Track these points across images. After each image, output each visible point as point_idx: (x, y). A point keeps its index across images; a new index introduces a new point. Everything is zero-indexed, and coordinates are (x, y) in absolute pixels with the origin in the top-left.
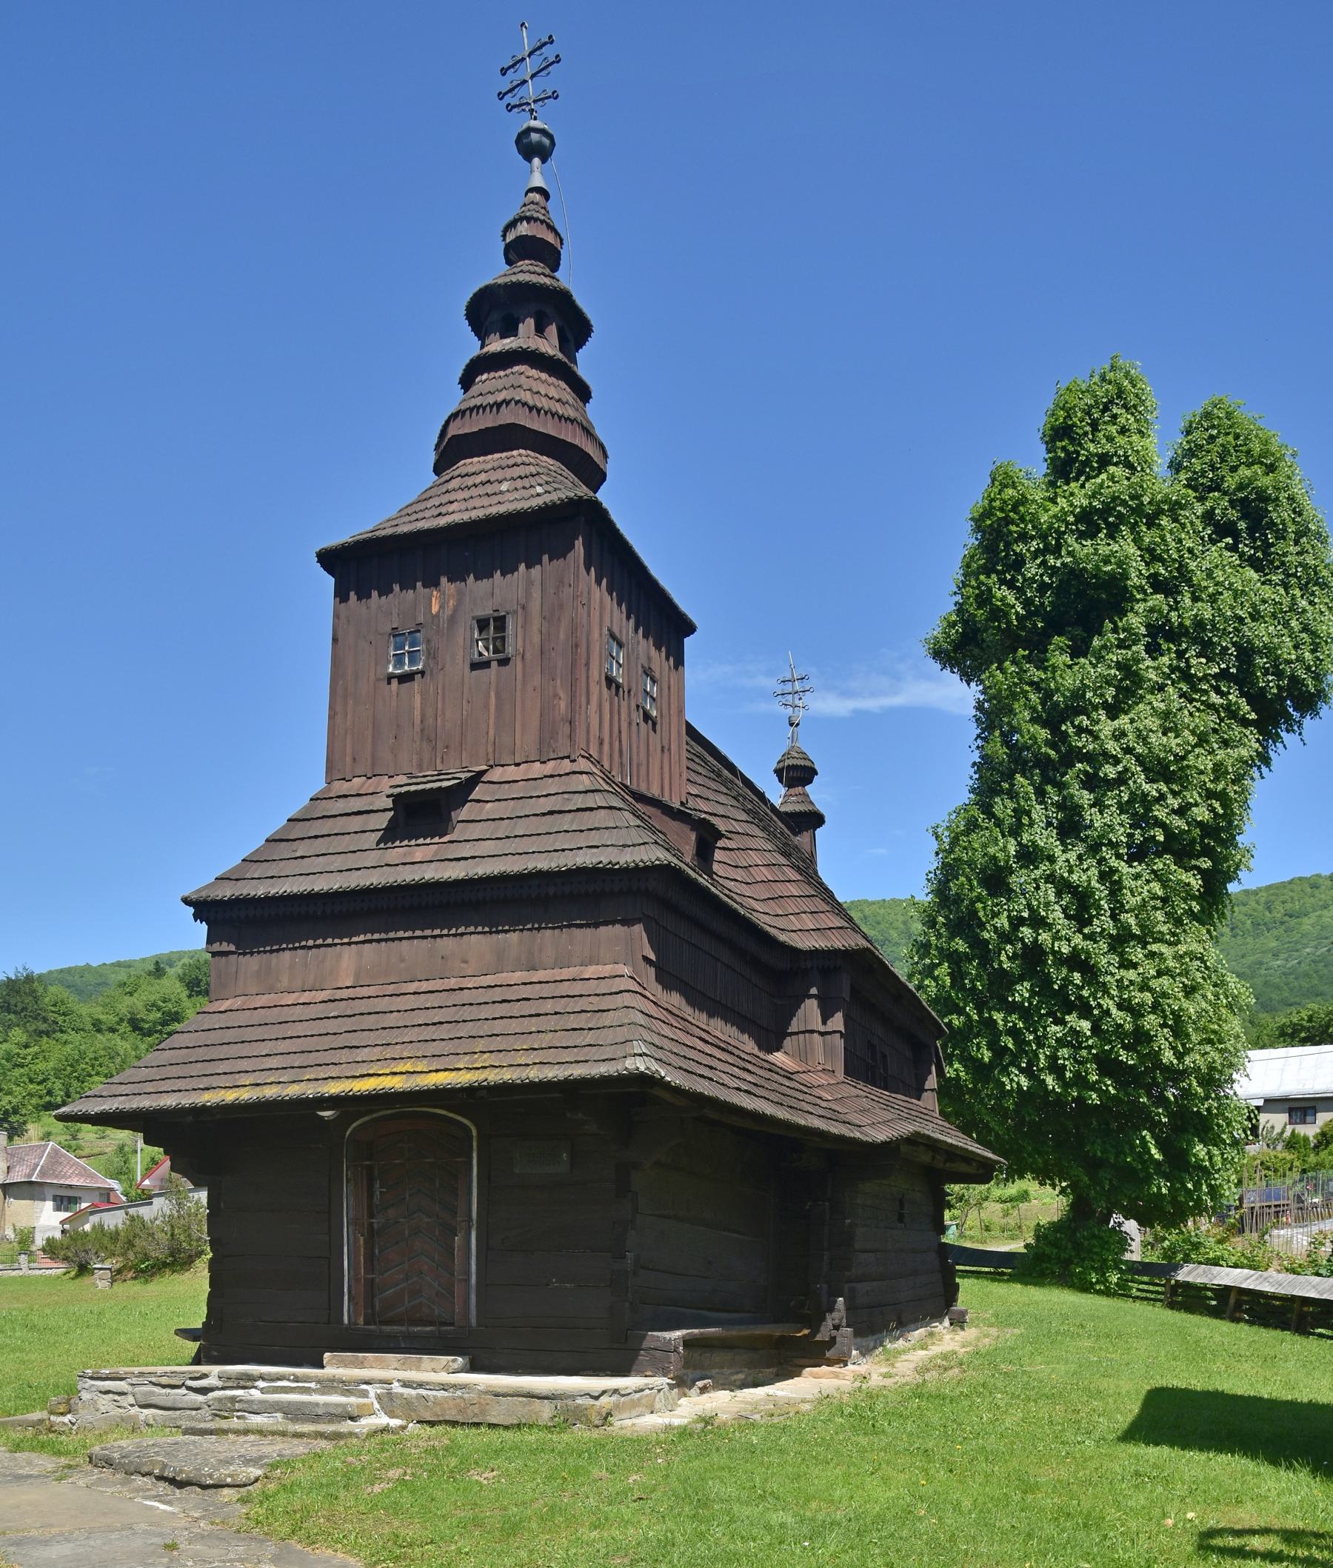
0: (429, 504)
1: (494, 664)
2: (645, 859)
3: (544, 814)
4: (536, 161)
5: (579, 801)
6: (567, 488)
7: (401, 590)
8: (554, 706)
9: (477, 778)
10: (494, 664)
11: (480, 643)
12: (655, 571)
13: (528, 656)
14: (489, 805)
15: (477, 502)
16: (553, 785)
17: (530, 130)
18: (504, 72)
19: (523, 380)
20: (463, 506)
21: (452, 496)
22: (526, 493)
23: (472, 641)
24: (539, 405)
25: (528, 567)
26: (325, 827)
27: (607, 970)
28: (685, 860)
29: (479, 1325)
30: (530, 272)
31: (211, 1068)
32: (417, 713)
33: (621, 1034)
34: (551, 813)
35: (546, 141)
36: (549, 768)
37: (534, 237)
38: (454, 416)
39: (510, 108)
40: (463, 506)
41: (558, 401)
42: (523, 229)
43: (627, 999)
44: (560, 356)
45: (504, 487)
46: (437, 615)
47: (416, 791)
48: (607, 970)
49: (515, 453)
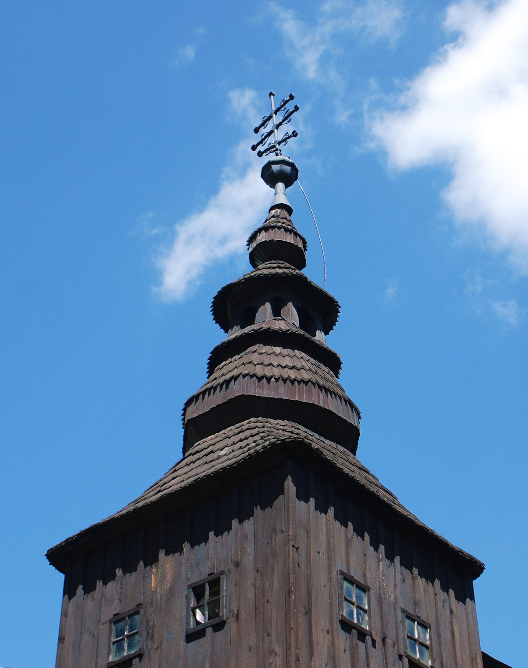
1: (209, 631)
4: (280, 186)
7: (124, 573)
8: (271, 664)
10: (209, 631)
11: (198, 612)
13: (243, 615)
17: (270, 164)
18: (256, 130)
23: (187, 609)
24: (268, 374)
25: (241, 522)
35: (288, 169)
37: (272, 241)
38: (188, 403)
41: (293, 368)
42: (262, 237)
44: (302, 332)
49: (244, 423)
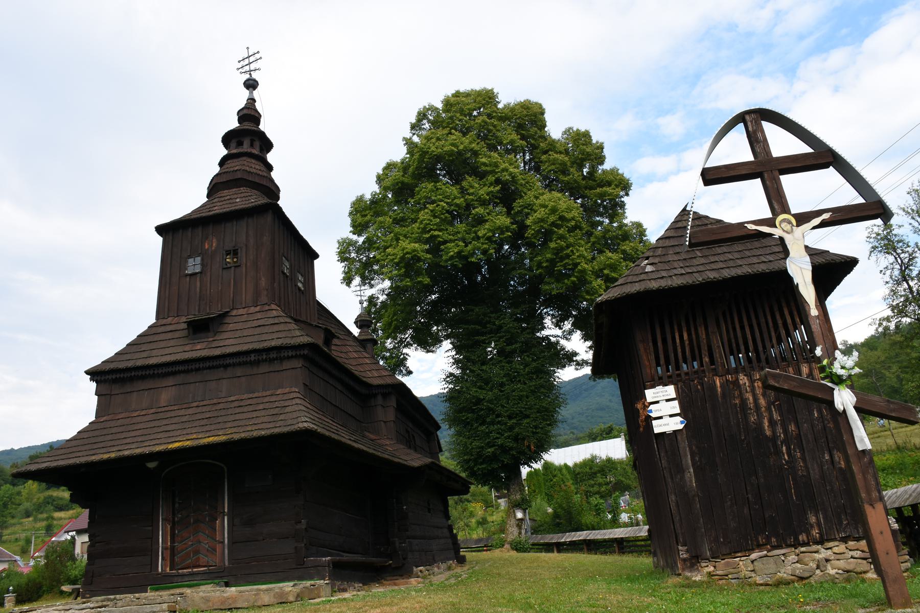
0: (205, 208)
2: (303, 341)
3: (256, 327)
5: (271, 321)
6: (263, 200)
9: (225, 315)
12: (302, 232)
14: (231, 325)
15: (226, 206)
16: (259, 316)
18: (239, 62)
19: (245, 162)
20: (220, 207)
21: (215, 205)
22: (247, 202)
26: (156, 338)
27: (287, 390)
28: (320, 342)
29: (229, 564)
30: (248, 126)
31: (95, 446)
32: (198, 289)
33: (295, 415)
34: (259, 326)
36: (258, 309)
39: (241, 73)
40: (220, 207)
43: (298, 401)
45: (238, 200)
46: (208, 249)
47: (198, 320)
48: (287, 390)
49: (242, 189)
